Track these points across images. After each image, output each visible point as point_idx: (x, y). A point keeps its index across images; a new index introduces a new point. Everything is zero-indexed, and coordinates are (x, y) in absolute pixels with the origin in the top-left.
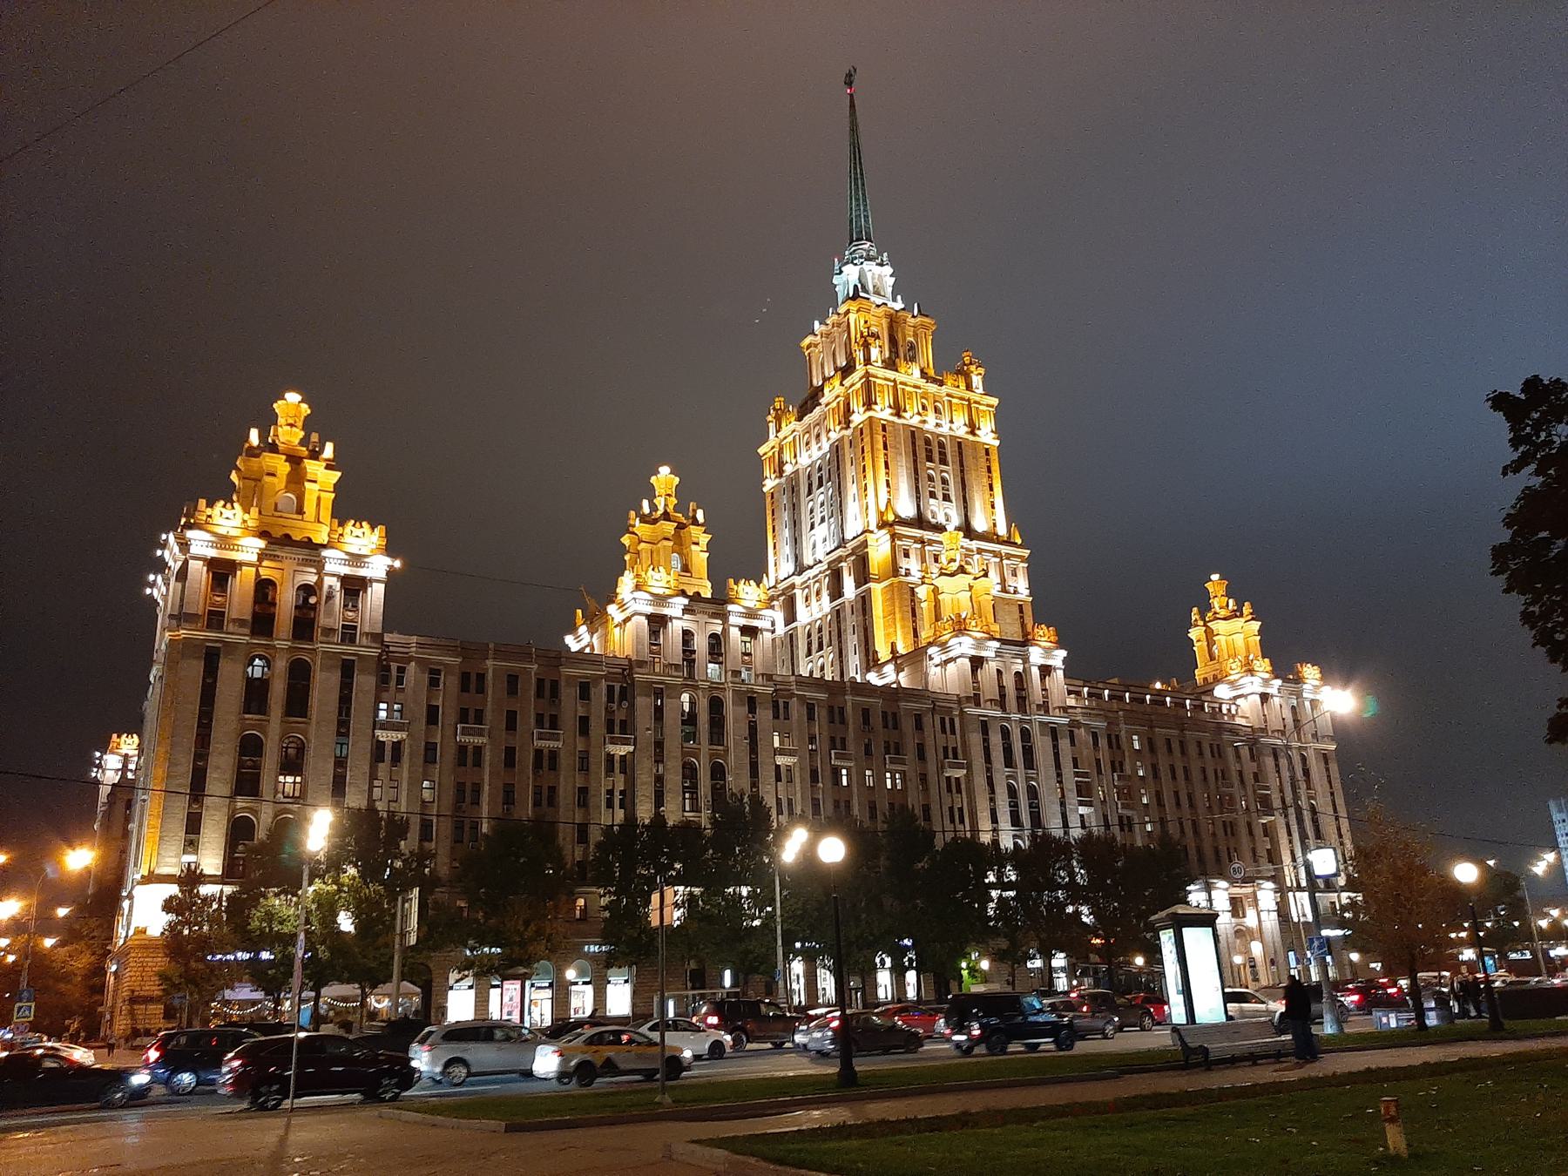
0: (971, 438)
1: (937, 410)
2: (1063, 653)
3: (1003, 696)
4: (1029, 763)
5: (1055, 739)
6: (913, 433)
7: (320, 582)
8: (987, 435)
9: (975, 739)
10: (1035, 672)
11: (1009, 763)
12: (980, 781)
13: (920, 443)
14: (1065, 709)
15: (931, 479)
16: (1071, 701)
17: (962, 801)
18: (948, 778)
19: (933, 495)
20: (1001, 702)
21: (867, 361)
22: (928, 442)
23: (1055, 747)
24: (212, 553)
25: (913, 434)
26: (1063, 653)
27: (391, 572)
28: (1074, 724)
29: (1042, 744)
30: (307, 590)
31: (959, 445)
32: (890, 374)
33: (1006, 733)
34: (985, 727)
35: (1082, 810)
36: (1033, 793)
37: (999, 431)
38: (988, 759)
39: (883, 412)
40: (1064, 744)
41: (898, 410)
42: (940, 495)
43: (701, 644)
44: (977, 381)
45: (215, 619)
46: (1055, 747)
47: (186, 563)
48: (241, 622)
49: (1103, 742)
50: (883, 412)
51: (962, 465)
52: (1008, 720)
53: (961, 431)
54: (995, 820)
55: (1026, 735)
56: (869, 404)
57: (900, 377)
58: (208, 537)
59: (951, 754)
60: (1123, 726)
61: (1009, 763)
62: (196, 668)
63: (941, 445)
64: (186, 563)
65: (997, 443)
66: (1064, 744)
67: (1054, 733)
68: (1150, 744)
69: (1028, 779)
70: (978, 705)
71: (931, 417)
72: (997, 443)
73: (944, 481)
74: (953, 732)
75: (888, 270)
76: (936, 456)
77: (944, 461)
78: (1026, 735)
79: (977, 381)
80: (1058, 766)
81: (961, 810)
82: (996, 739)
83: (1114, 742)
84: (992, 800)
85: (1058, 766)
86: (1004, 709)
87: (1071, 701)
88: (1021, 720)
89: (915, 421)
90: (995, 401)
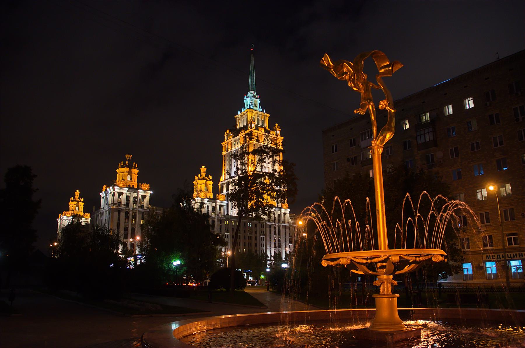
2: (289, 210)
4: (279, 234)
5: (285, 229)
7: (138, 196)
9: (268, 229)
10: (283, 214)
11: (275, 234)
12: (268, 238)
14: (288, 222)
16: (290, 220)
17: (264, 242)
20: (274, 221)
23: (285, 231)
24: (118, 191)
26: (289, 210)
27: (150, 194)
28: (290, 226)
29: (282, 230)
30: (135, 198)
34: (270, 226)
36: (279, 240)
38: (270, 234)
40: (287, 230)
43: (210, 209)
45: (119, 204)
46: (285, 231)
47: (114, 193)
48: (124, 205)
54: (270, 246)
55: (279, 228)
58: (118, 188)
59: (262, 233)
61: (275, 234)
62: (116, 214)
64: (114, 193)
66: (287, 230)
67: (285, 227)
75: (258, 100)
78: (279, 228)
80: (285, 235)
82: (273, 229)
85: (285, 235)
87: (290, 220)
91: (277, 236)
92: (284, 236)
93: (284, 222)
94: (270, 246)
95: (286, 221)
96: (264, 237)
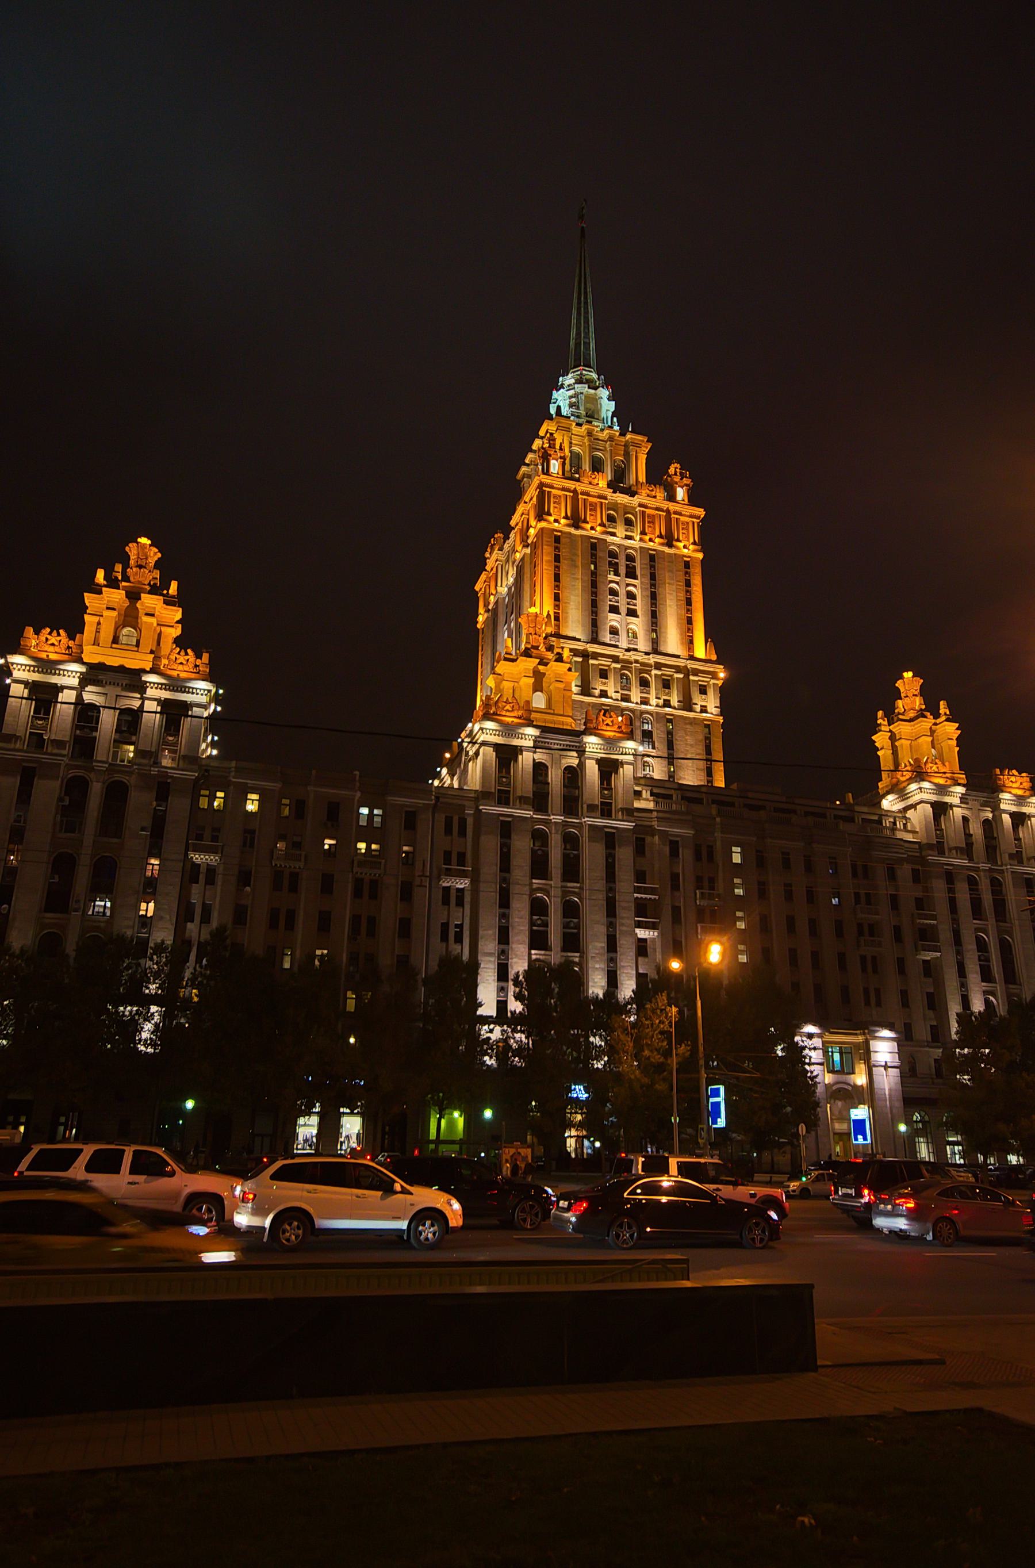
0: (666, 550)
1: (629, 523)
3: (969, 845)
6: (594, 546)
8: (688, 548)
9: (490, 844)
10: (592, 769)
13: (601, 554)
14: (630, 812)
15: (613, 593)
17: (461, 917)
18: (447, 890)
19: (614, 610)
20: (540, 800)
21: (547, 472)
22: (613, 555)
25: (594, 547)
29: (592, 855)
31: (652, 558)
32: (571, 485)
33: (972, 882)
34: (506, 828)
35: (642, 933)
37: (704, 543)
38: (505, 866)
39: (558, 522)
41: (576, 521)
42: (623, 610)
44: (681, 493)
49: (686, 854)
50: (558, 522)
51: (653, 577)
52: (976, 870)
53: (656, 545)
56: (541, 514)
57: (580, 487)
59: (455, 861)
60: (718, 834)
63: (630, 558)
65: (700, 556)
66: (625, 854)
67: (610, 839)
68: (757, 859)
69: (565, 893)
70: (941, 853)
71: (621, 530)
72: (700, 556)
73: (631, 596)
74: (462, 832)
76: (622, 570)
77: (631, 574)
79: (681, 493)
81: (460, 926)
82: (522, 846)
83: (706, 855)
84: (504, 916)
86: (971, 859)
88: (565, 824)
89: (598, 533)
90: (701, 512)
91: (556, 881)
92: (601, 885)
93: (606, 810)
94: (504, 938)
95: (620, 800)
96: (463, 884)
